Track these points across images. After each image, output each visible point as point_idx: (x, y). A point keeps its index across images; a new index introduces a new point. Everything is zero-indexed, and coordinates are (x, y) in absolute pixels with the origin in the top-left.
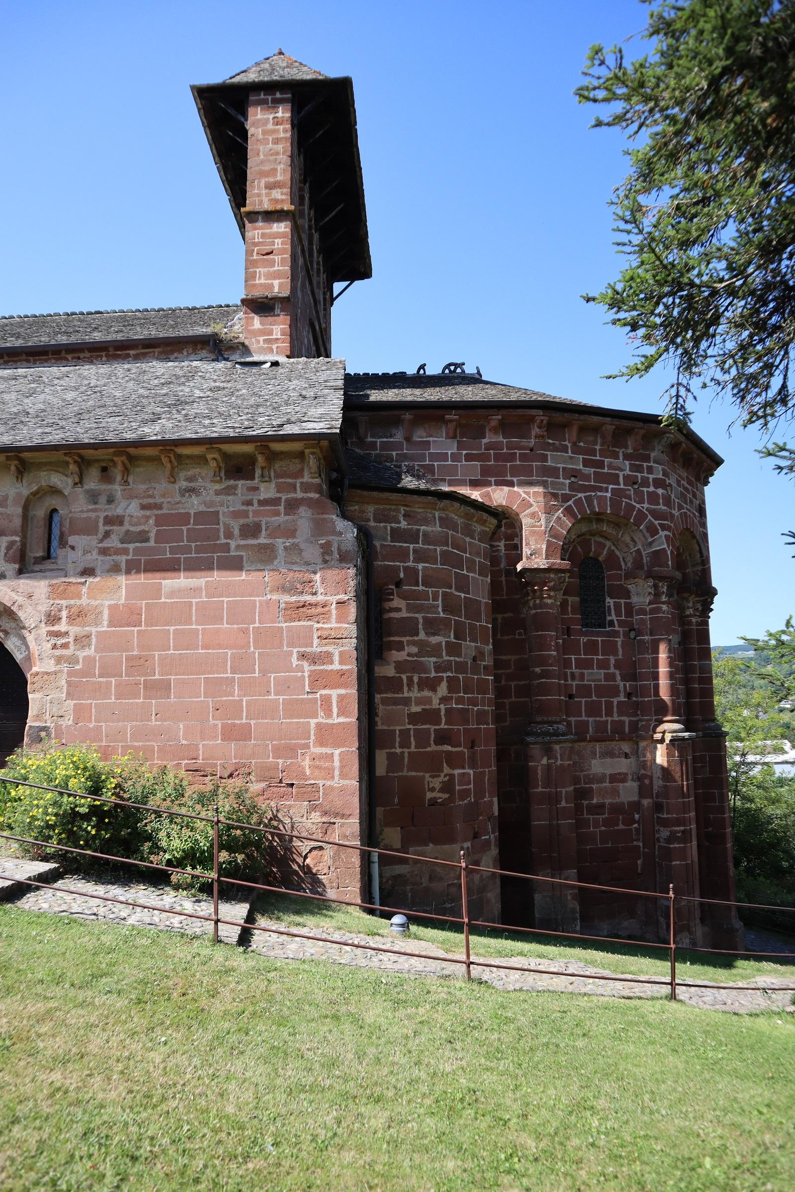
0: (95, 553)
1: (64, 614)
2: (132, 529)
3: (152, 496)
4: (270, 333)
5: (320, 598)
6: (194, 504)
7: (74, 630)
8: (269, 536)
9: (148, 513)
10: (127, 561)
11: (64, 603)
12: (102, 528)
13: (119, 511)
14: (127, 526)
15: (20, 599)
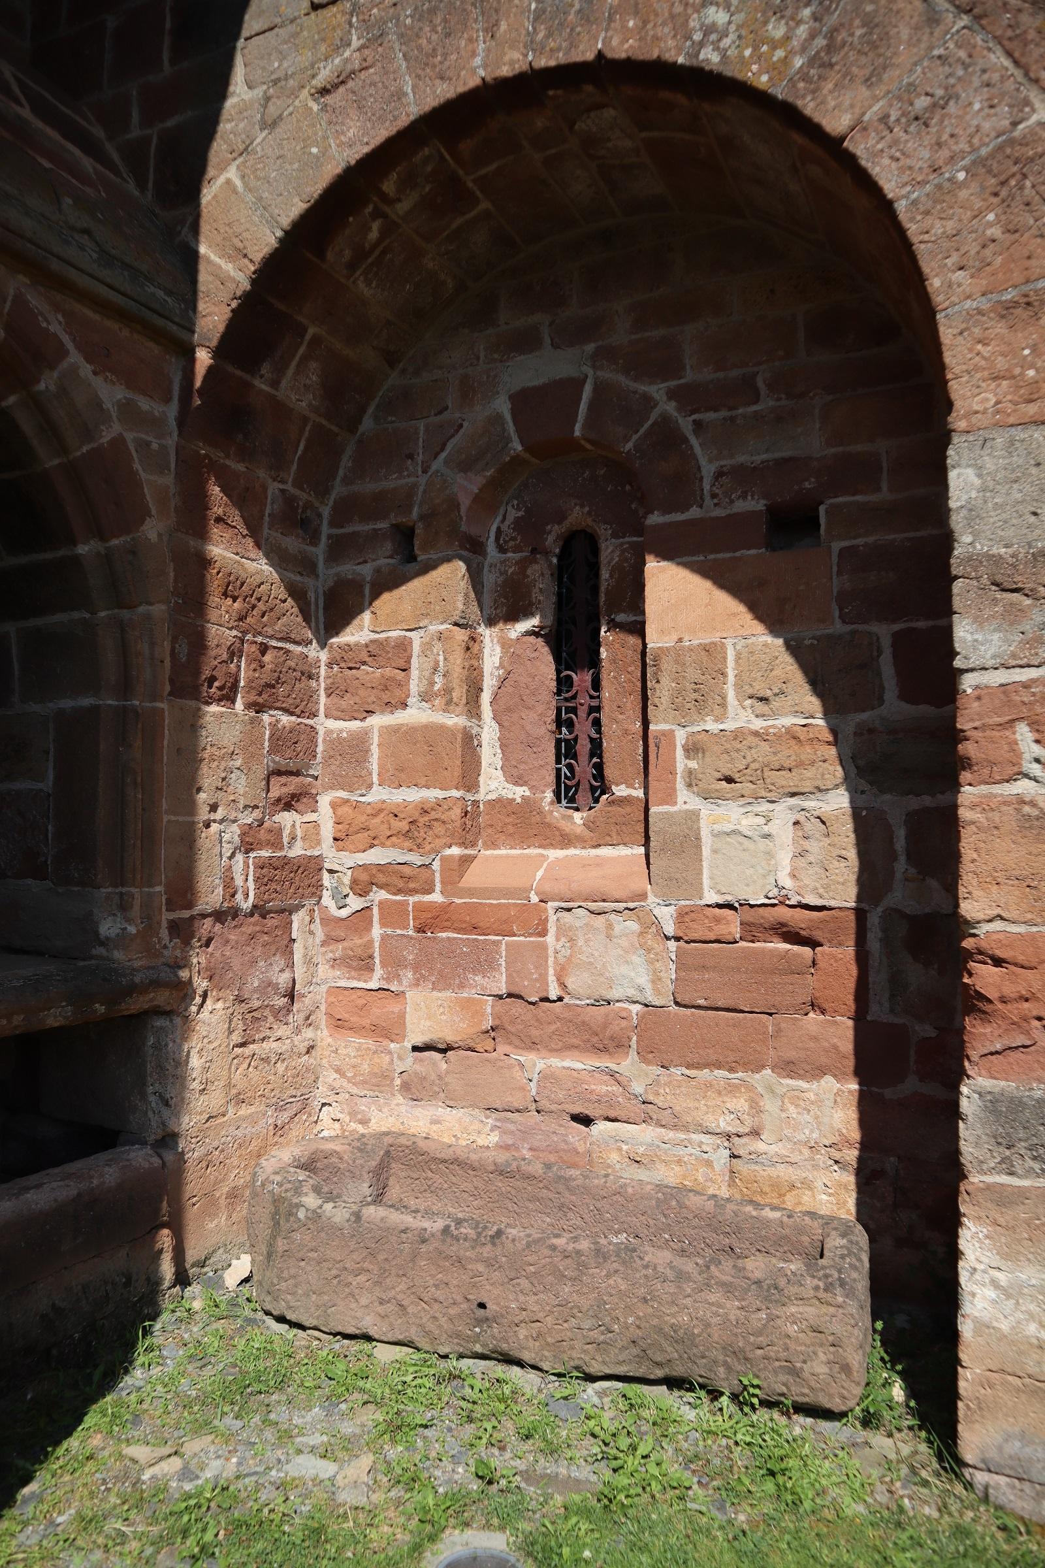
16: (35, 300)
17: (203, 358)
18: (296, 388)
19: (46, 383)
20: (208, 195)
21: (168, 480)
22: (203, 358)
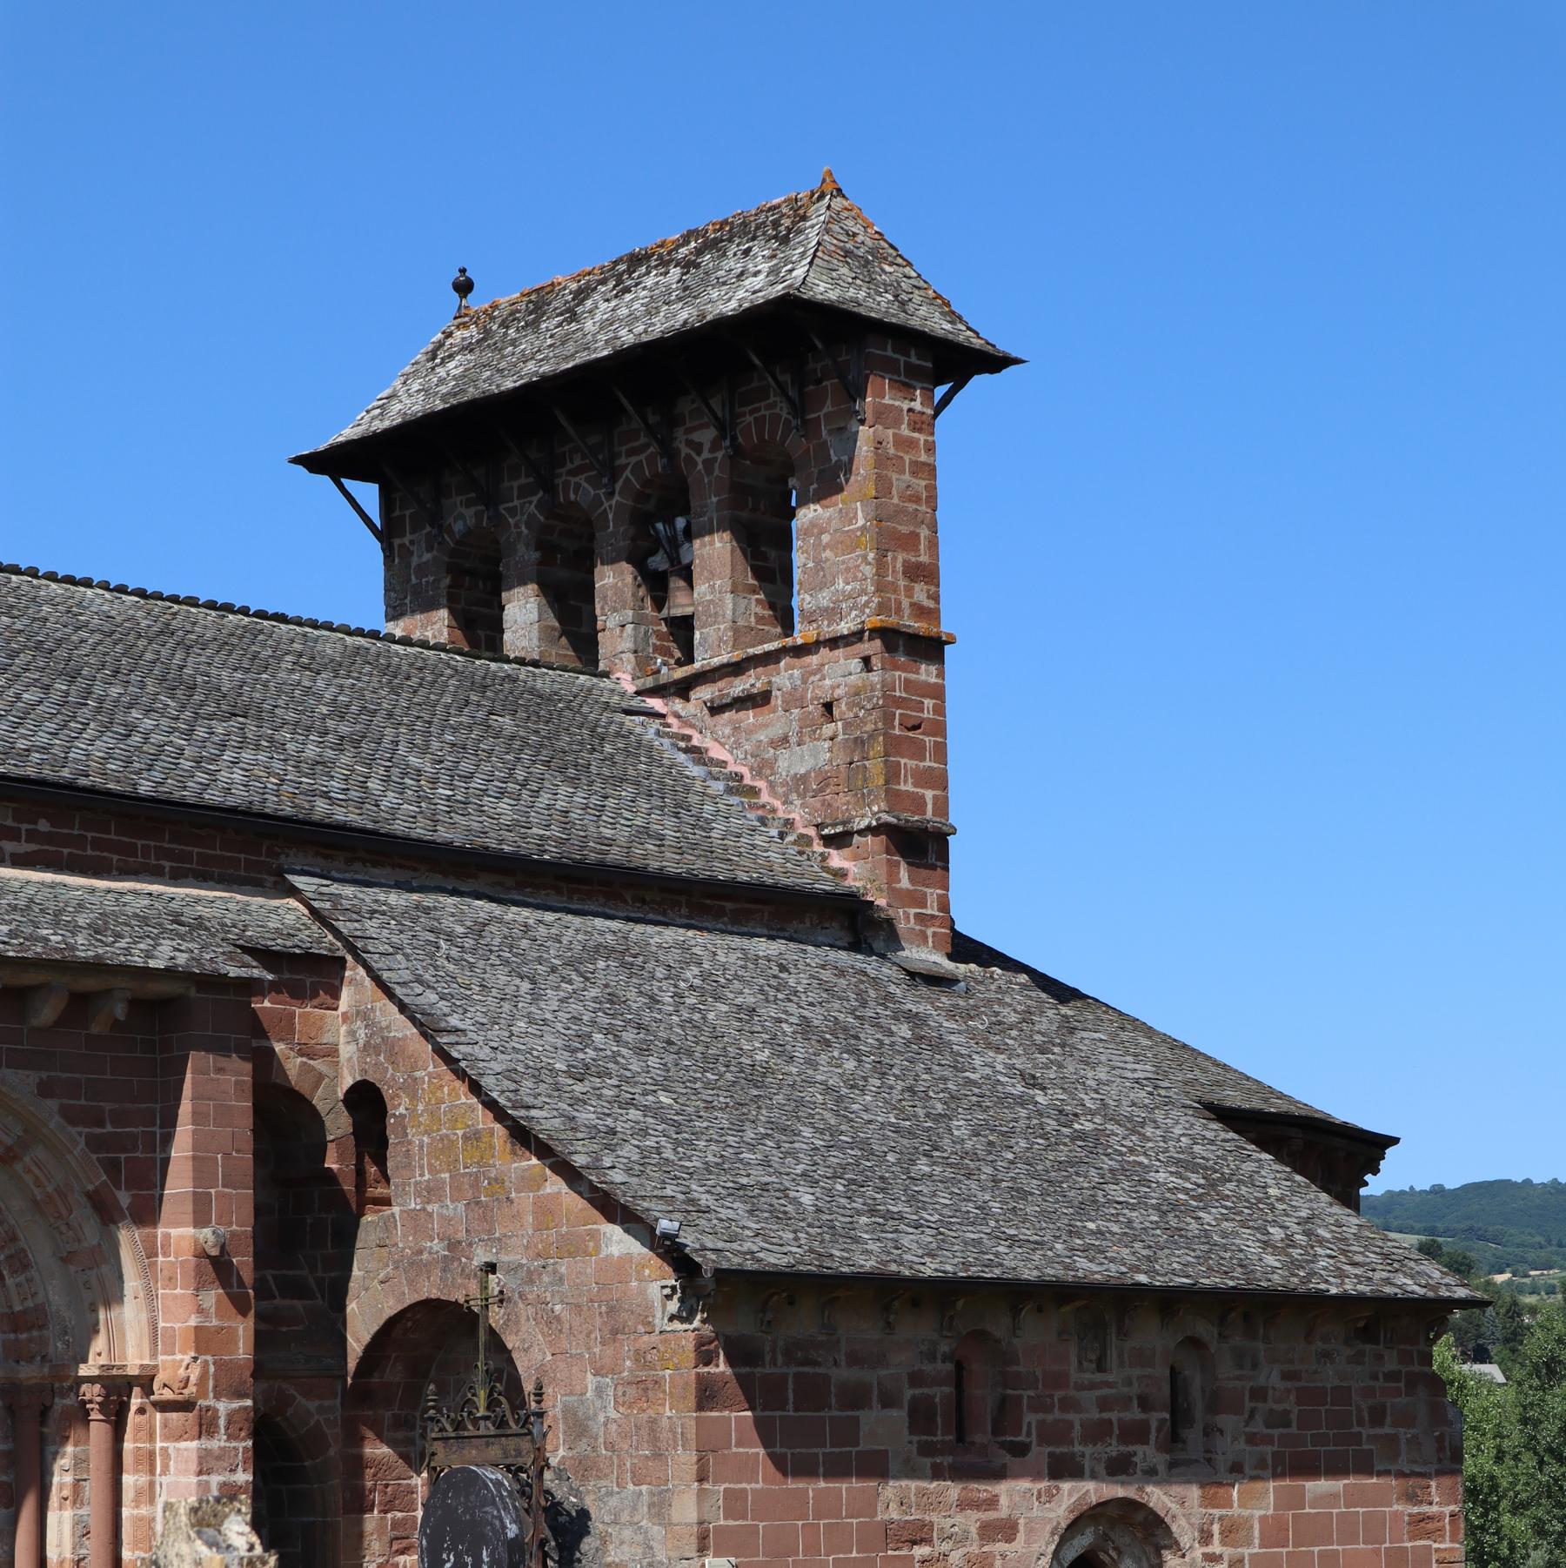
0: (1242, 1439)
1: (1216, 1528)
2: (1275, 1407)
3: (1291, 1361)
4: (922, 903)
5: (1435, 1508)
6: (1329, 1377)
7: (1227, 1552)
8: (1395, 1425)
9: (1289, 1384)
10: (1273, 1453)
11: (1217, 1512)
12: (1248, 1405)
13: (1261, 1381)
14: (1271, 1404)
15: (1174, 1507)
16: (284, 1386)
17: (349, 1381)
18: (393, 1374)
19: (290, 1412)
20: (349, 1310)
21: (338, 1430)
22: (349, 1381)
